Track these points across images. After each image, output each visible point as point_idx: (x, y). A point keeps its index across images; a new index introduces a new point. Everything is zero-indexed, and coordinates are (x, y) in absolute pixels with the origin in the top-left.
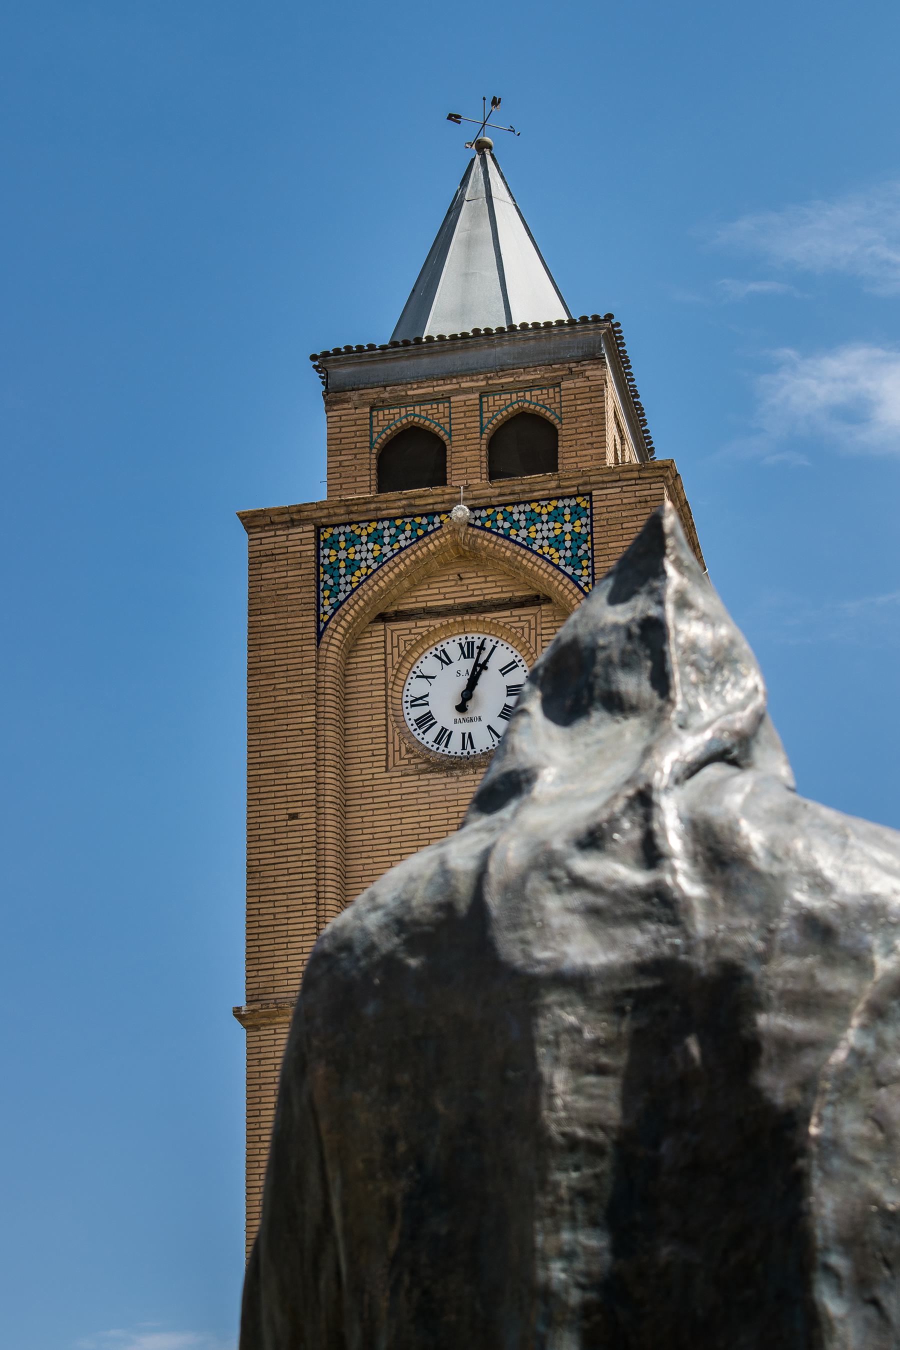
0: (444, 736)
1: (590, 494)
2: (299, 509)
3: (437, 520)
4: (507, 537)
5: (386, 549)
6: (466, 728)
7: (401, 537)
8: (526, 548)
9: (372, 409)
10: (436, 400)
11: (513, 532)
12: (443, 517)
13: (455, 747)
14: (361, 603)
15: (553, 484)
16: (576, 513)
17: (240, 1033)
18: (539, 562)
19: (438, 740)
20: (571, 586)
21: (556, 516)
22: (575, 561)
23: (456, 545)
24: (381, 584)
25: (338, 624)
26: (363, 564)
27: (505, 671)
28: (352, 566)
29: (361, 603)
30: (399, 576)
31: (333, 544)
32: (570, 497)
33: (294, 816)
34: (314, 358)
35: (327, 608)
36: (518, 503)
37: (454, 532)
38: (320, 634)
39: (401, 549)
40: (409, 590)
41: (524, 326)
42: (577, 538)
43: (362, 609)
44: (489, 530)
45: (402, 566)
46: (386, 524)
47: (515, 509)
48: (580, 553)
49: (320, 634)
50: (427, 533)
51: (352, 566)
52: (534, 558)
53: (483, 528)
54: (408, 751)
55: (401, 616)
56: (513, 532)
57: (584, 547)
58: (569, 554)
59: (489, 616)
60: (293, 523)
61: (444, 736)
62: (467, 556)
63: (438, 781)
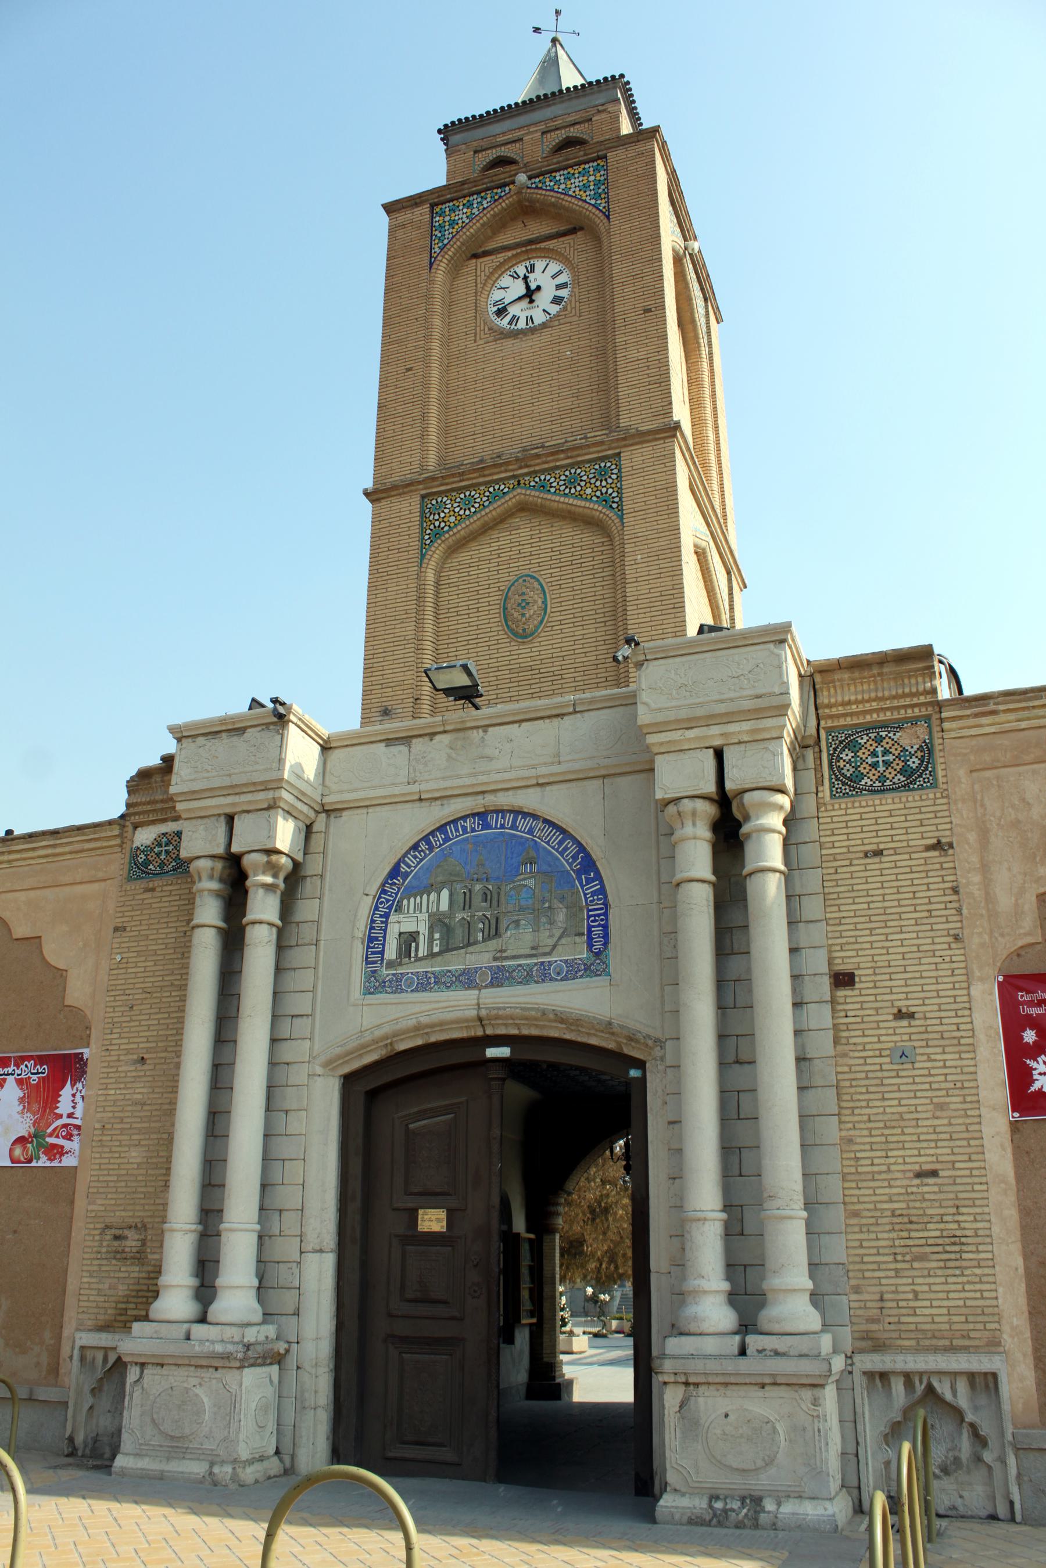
0: (515, 319)
1: (606, 157)
2: (420, 196)
3: (507, 189)
4: (552, 190)
5: (475, 211)
6: (528, 313)
7: (485, 202)
8: (565, 194)
9: (476, 152)
10: (514, 141)
11: (556, 187)
12: (511, 186)
13: (522, 324)
14: (458, 243)
15: (582, 153)
16: (597, 169)
17: (367, 506)
18: (573, 200)
19: (510, 323)
20: (594, 210)
21: (585, 173)
22: (597, 196)
23: (520, 202)
24: (472, 230)
25: (443, 257)
26: (460, 222)
27: (554, 277)
28: (452, 223)
29: (458, 243)
30: (483, 225)
31: (442, 214)
32: (593, 161)
33: (410, 369)
34: (439, 131)
35: (437, 250)
36: (559, 171)
37: (519, 193)
38: (431, 265)
39: (484, 209)
40: (491, 237)
41: (568, 89)
42: (597, 183)
43: (459, 247)
44: (541, 188)
45: (485, 219)
46: (475, 197)
47: (558, 174)
48: (600, 191)
49: (431, 265)
50: (500, 197)
51: (452, 223)
52: (569, 199)
53: (537, 188)
54: (489, 329)
55: (486, 254)
56: (556, 187)
57: (603, 187)
58: (592, 193)
59: (543, 245)
60: (417, 205)
61: (515, 319)
62: (527, 209)
63: (508, 343)
